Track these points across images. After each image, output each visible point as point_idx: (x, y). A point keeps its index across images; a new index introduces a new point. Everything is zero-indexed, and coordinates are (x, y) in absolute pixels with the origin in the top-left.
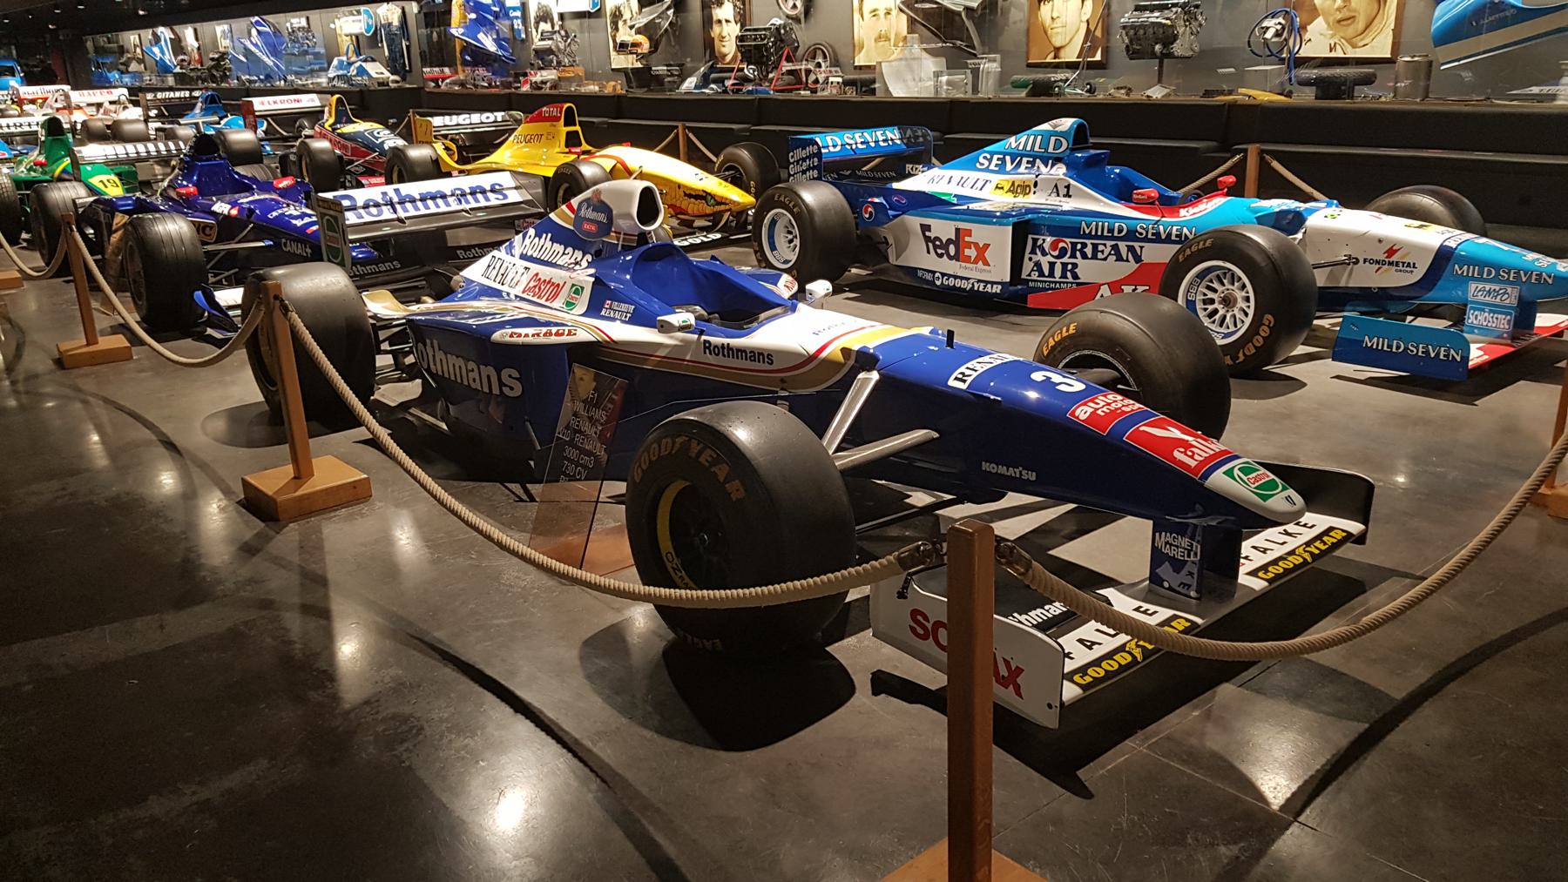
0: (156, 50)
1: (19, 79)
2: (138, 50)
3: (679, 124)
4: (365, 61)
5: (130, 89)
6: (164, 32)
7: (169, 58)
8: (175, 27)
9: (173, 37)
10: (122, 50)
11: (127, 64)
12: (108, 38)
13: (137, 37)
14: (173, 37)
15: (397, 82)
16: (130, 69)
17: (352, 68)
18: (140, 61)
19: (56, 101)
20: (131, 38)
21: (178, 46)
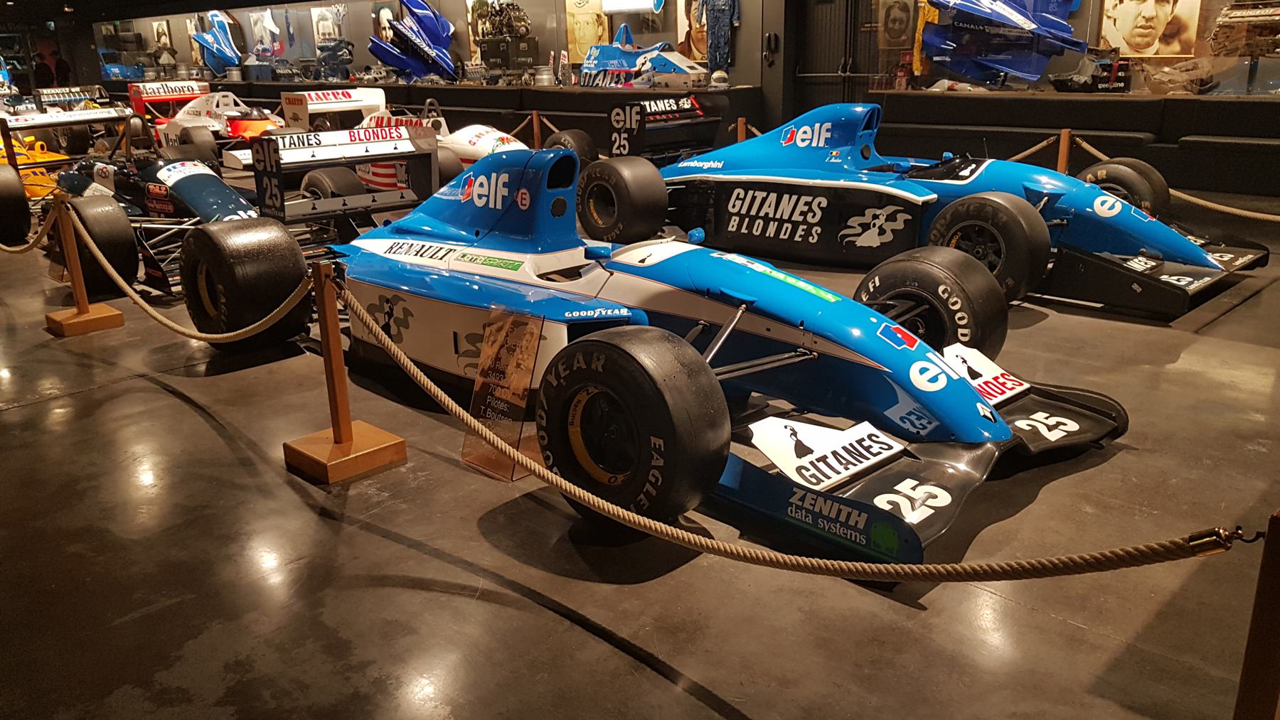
0: (209, 38)
1: (5, 72)
2: (165, 40)
3: (534, 112)
4: (663, 50)
5: (388, 90)
6: (217, 16)
7: (230, 51)
8: (229, 11)
9: (231, 22)
10: (140, 42)
11: (156, 56)
12: (115, 27)
13: (165, 23)
14: (231, 22)
15: (724, 80)
16: (161, 61)
17: (640, 60)
18: (173, 52)
19: (218, 106)
20: (154, 26)
21: (239, 33)
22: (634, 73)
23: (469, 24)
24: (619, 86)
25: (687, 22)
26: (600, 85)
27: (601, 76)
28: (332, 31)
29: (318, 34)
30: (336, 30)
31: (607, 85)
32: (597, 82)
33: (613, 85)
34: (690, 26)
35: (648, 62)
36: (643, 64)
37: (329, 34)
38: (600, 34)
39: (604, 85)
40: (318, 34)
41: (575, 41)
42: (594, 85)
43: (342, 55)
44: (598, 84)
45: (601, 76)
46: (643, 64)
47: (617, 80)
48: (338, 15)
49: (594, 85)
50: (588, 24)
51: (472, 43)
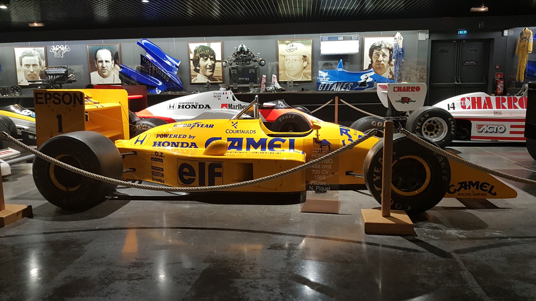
22: (360, 83)
23: (191, 60)
24: (347, 90)
25: (370, 60)
26: (335, 90)
27: (335, 85)
28: (38, 63)
29: (21, 65)
30: (43, 63)
31: (339, 90)
32: (333, 88)
33: (343, 90)
34: (372, 61)
35: (369, 78)
36: (366, 79)
37: (34, 65)
38: (305, 66)
39: (337, 90)
40: (21, 65)
41: (285, 69)
42: (331, 90)
43: (71, 77)
44: (333, 90)
45: (335, 85)
46: (366, 79)
47: (345, 87)
48: (59, 52)
49: (331, 90)
50: (296, 61)
51: (192, 71)
